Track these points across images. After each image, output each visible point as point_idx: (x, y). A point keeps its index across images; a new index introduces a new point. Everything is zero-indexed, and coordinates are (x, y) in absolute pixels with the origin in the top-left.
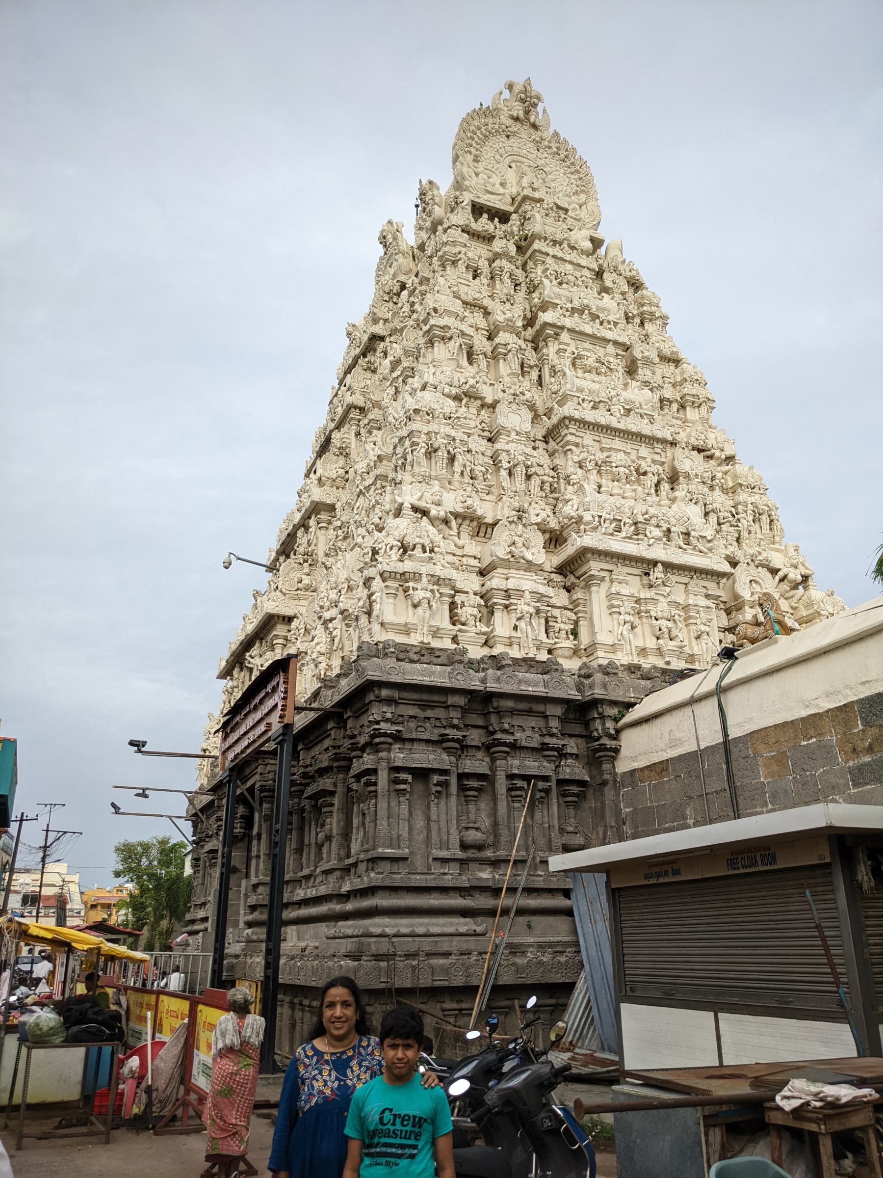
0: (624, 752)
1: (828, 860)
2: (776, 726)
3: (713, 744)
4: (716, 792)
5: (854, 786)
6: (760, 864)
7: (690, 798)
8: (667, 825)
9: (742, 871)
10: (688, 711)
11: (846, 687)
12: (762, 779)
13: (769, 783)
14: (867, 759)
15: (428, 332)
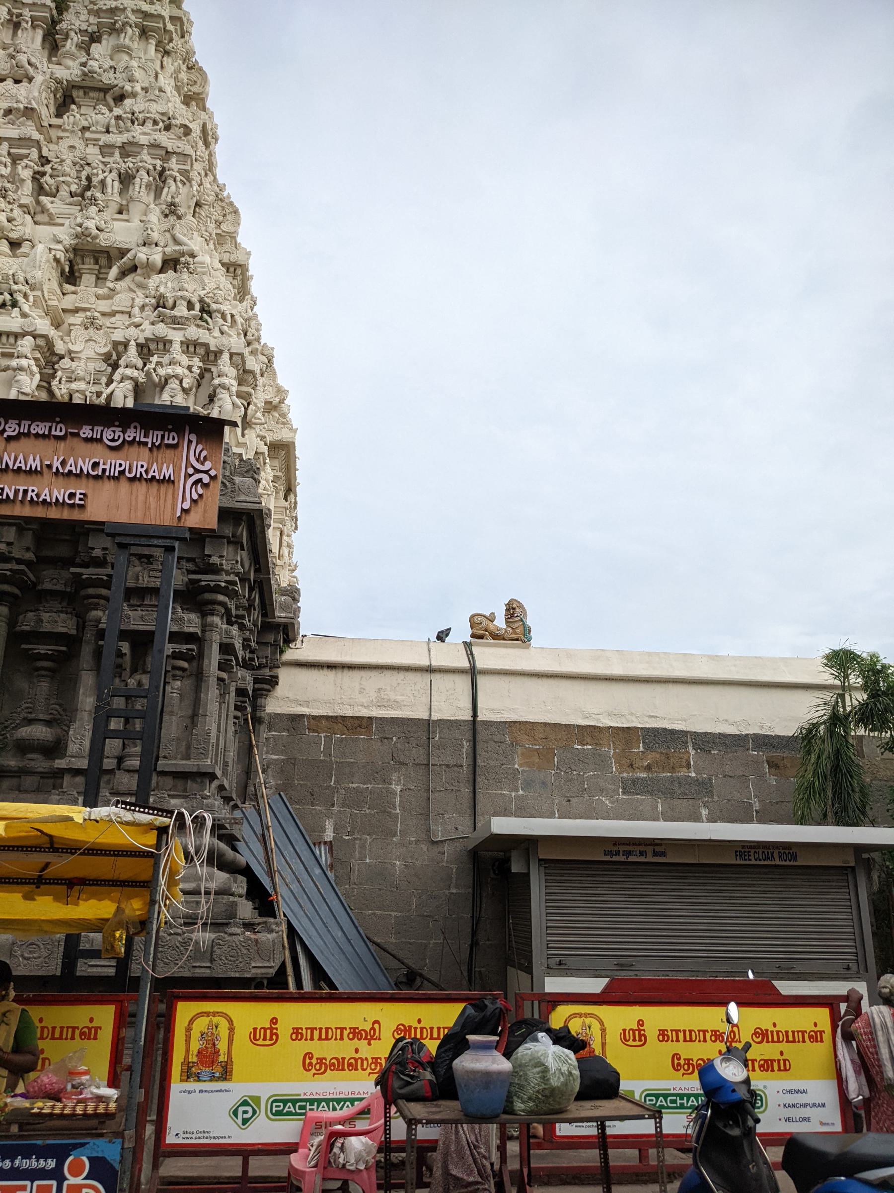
0: (281, 690)
1: (852, 864)
2: (546, 724)
3: (452, 718)
4: (447, 766)
5: (624, 793)
6: (777, 858)
7: (401, 763)
8: (355, 785)
9: (753, 862)
10: (427, 677)
11: (632, 714)
12: (516, 766)
13: (524, 771)
14: (644, 775)
15: (146, 15)
